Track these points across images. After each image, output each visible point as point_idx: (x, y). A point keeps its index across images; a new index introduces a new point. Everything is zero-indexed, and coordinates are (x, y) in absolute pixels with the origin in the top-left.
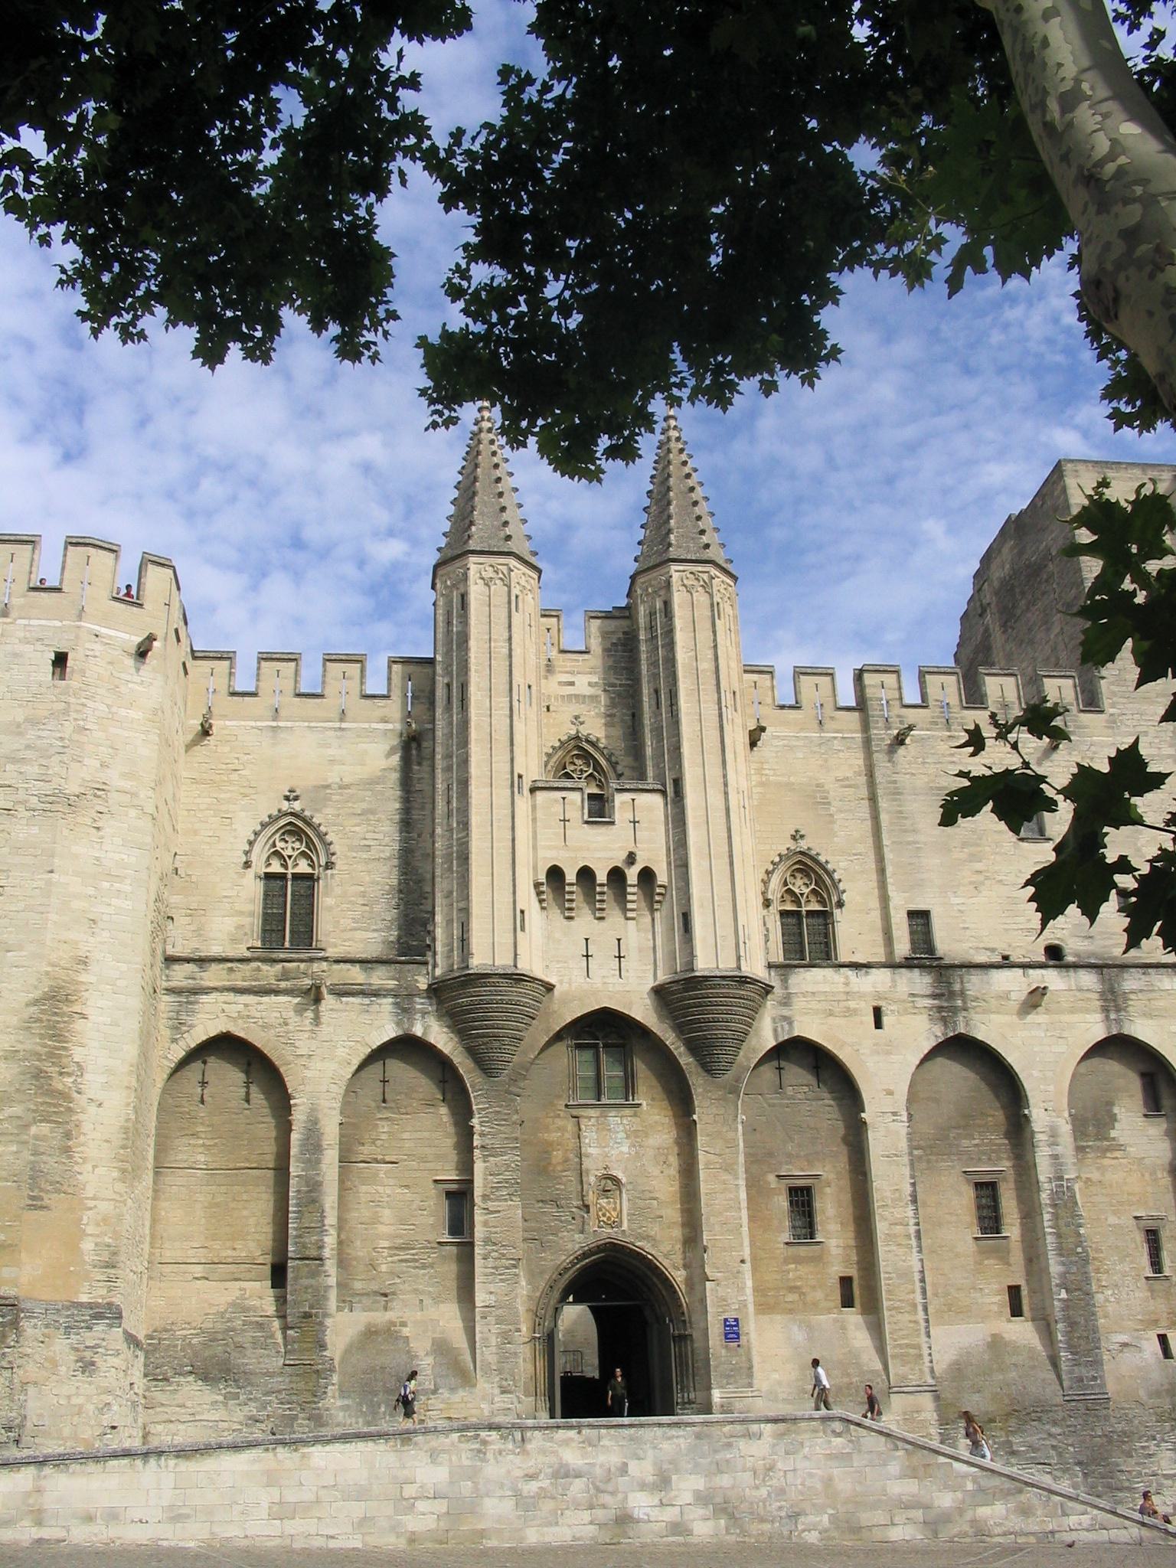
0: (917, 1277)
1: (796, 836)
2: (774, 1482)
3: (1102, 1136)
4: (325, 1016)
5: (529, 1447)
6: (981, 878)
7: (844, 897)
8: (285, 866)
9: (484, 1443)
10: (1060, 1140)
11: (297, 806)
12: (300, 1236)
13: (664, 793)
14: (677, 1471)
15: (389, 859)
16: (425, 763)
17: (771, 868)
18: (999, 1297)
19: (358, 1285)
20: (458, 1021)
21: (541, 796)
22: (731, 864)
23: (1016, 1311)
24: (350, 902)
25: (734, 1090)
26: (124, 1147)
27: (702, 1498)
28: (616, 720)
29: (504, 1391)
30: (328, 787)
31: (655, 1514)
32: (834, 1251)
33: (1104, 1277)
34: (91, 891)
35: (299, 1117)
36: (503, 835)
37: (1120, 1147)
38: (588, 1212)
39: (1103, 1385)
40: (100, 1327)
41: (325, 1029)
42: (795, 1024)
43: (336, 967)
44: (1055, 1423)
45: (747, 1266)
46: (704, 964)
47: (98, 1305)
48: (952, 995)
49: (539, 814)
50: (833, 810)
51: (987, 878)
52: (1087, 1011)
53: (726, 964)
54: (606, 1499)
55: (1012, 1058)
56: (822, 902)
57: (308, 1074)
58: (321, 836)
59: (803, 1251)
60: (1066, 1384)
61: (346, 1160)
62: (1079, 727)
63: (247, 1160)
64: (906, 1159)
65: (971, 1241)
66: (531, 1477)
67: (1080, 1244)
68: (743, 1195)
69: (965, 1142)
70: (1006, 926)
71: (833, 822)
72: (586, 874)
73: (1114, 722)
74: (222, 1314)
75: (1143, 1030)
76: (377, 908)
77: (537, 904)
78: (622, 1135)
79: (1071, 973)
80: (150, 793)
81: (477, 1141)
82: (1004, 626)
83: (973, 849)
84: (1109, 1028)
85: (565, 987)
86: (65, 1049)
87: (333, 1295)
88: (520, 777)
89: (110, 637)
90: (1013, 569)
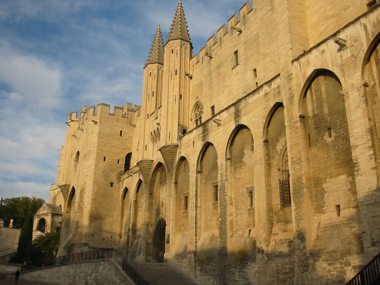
0: (194, 218)
1: (197, 98)
3: (241, 162)
27: (95, 278)
33: (238, 211)
37: (245, 164)
52: (231, 121)
64: (195, 185)
66: (80, 273)
70: (228, 101)
71: (203, 90)
75: (243, 121)
77: (151, 142)
79: (229, 110)
80: (96, 149)
86: (82, 199)
88: (148, 115)
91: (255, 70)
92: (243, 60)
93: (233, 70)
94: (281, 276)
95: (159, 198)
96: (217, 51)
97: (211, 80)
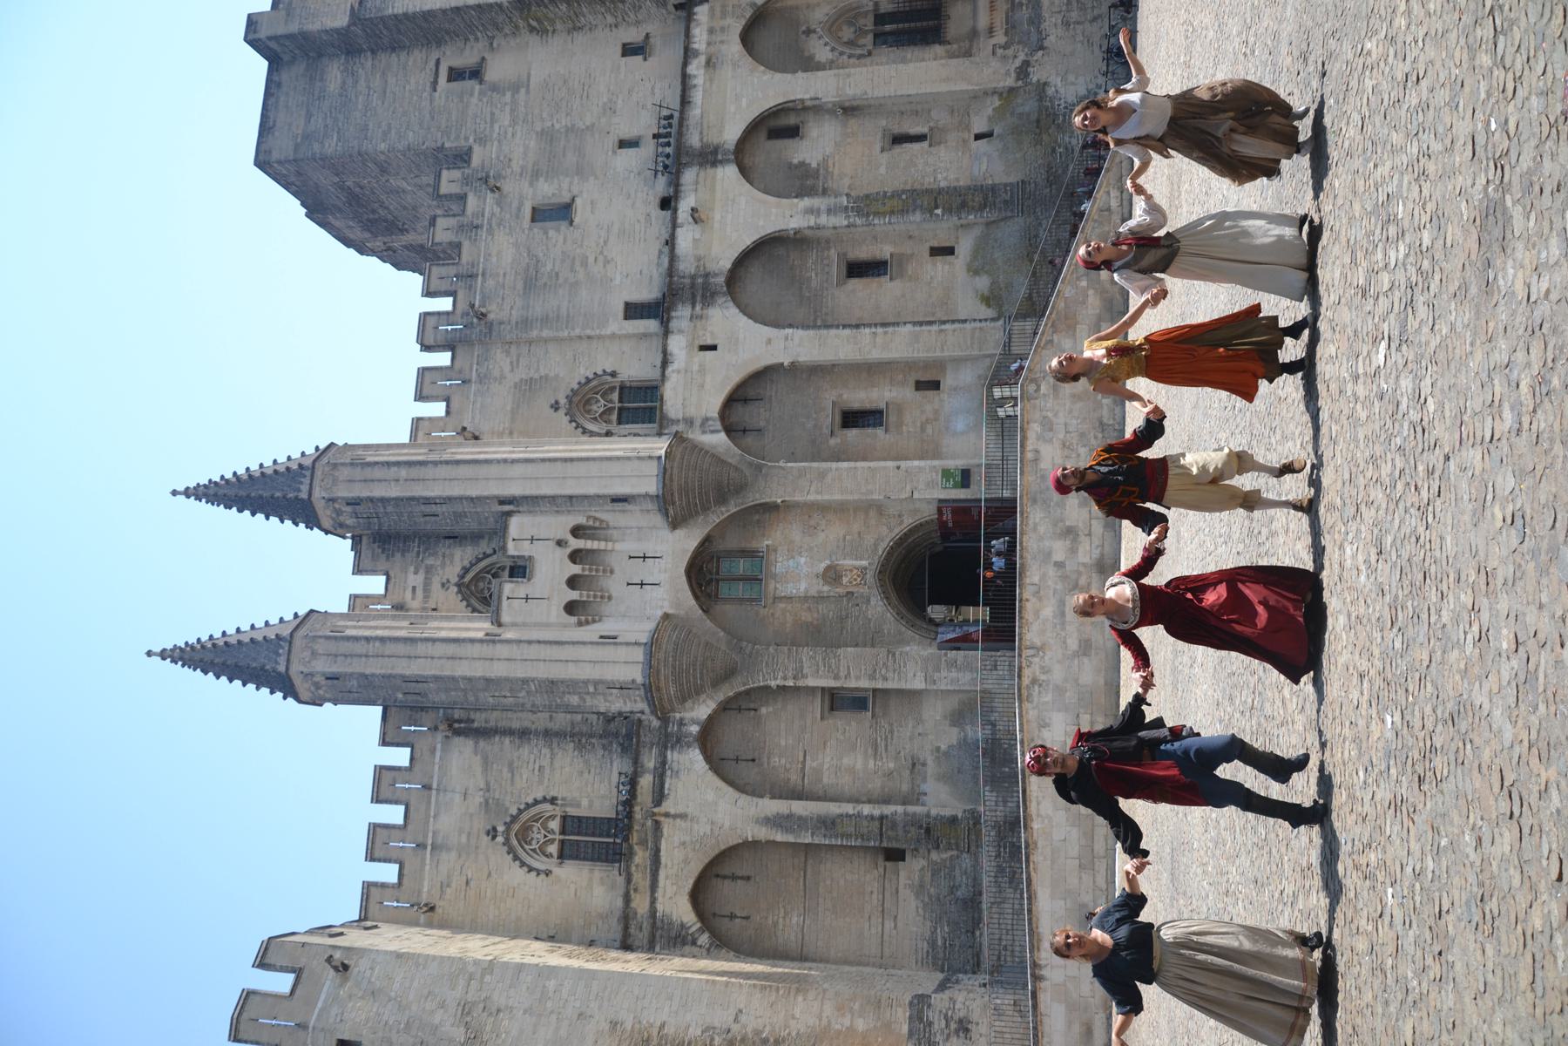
0: (917, 328)
1: (556, 407)
2: (1075, 442)
3: (815, 174)
4: (680, 809)
5: (1039, 644)
6: (601, 258)
7: (608, 371)
8: (552, 841)
9: (1034, 681)
10: (816, 206)
11: (501, 829)
12: (862, 836)
13: (509, 514)
14: (1062, 520)
15: (552, 749)
16: (472, 716)
17: (580, 430)
18: (939, 266)
19: (905, 787)
20: (689, 694)
21: (505, 618)
22: (571, 460)
23: (949, 251)
24: (586, 784)
25: (759, 468)
26: (778, 989)
28: (447, 552)
29: (995, 668)
30: (487, 802)
31: (1096, 542)
32: (894, 394)
33: (927, 179)
34: (554, 1017)
35: (763, 833)
36: (533, 652)
37: (825, 160)
38: (852, 593)
39: (1011, 184)
40: (931, 1015)
41: (689, 811)
42: (709, 415)
43: (639, 800)
44: (1040, 224)
45: (903, 464)
46: (651, 486)
47: (910, 1018)
48: (693, 285)
49: (519, 620)
50: (536, 376)
51: (601, 253)
52: (714, 178)
53: (653, 469)
54: (1083, 581)
55: (748, 241)
56: (612, 389)
57: (727, 824)
58: (528, 806)
59: (893, 418)
60: (1009, 214)
61: (799, 795)
62: (483, 168)
63: (798, 880)
64: (824, 332)
65: (890, 285)
67: (899, 196)
68: (845, 465)
69: (814, 284)
71: (547, 376)
72: (573, 582)
73: (481, 139)
74: (925, 905)
75: (731, 134)
76: (594, 762)
78: (791, 562)
79: (683, 188)
81: (790, 683)
82: (403, 231)
83: (577, 263)
84: (728, 161)
85: (666, 604)
87: (911, 809)
88: (487, 635)
89: (325, 1001)
90: (353, 219)
91: (623, 144)
92: (571, 183)
93: (577, 220)
94: (1074, 15)
95: (806, 598)
96: (482, 291)
97: (545, 321)
